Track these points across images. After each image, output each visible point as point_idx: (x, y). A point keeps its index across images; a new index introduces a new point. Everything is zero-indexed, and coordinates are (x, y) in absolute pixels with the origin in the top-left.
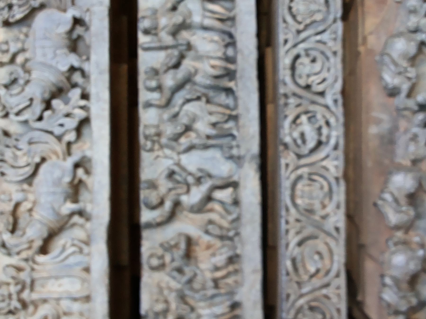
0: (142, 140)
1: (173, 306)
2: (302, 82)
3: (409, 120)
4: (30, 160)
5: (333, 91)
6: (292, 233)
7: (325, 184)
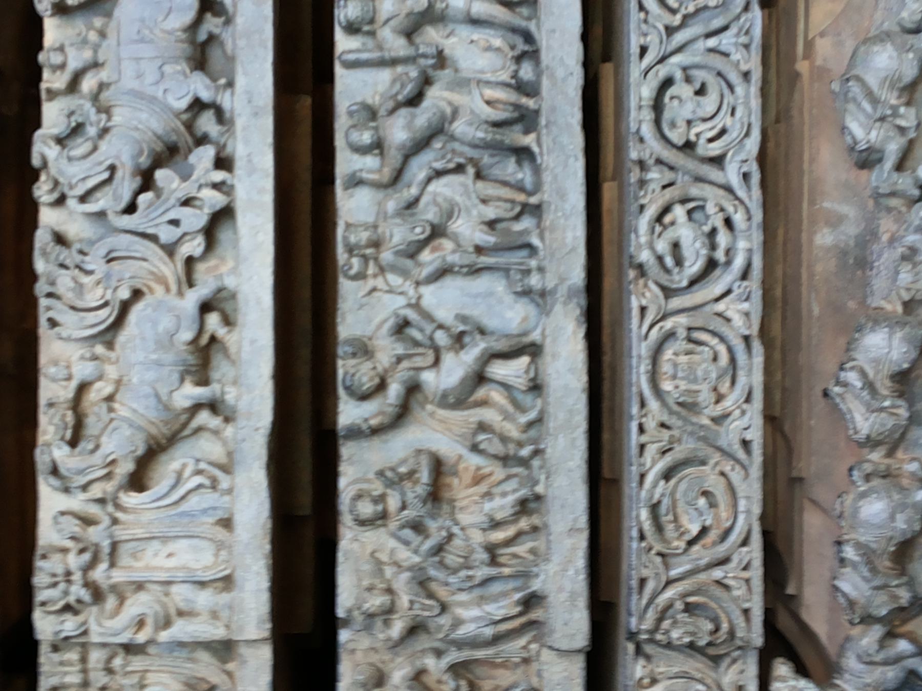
1: (404, 600)
2: (676, 136)
3: (900, 219)
4: (108, 297)
5: (743, 156)
6: (651, 450)
7: (722, 349)
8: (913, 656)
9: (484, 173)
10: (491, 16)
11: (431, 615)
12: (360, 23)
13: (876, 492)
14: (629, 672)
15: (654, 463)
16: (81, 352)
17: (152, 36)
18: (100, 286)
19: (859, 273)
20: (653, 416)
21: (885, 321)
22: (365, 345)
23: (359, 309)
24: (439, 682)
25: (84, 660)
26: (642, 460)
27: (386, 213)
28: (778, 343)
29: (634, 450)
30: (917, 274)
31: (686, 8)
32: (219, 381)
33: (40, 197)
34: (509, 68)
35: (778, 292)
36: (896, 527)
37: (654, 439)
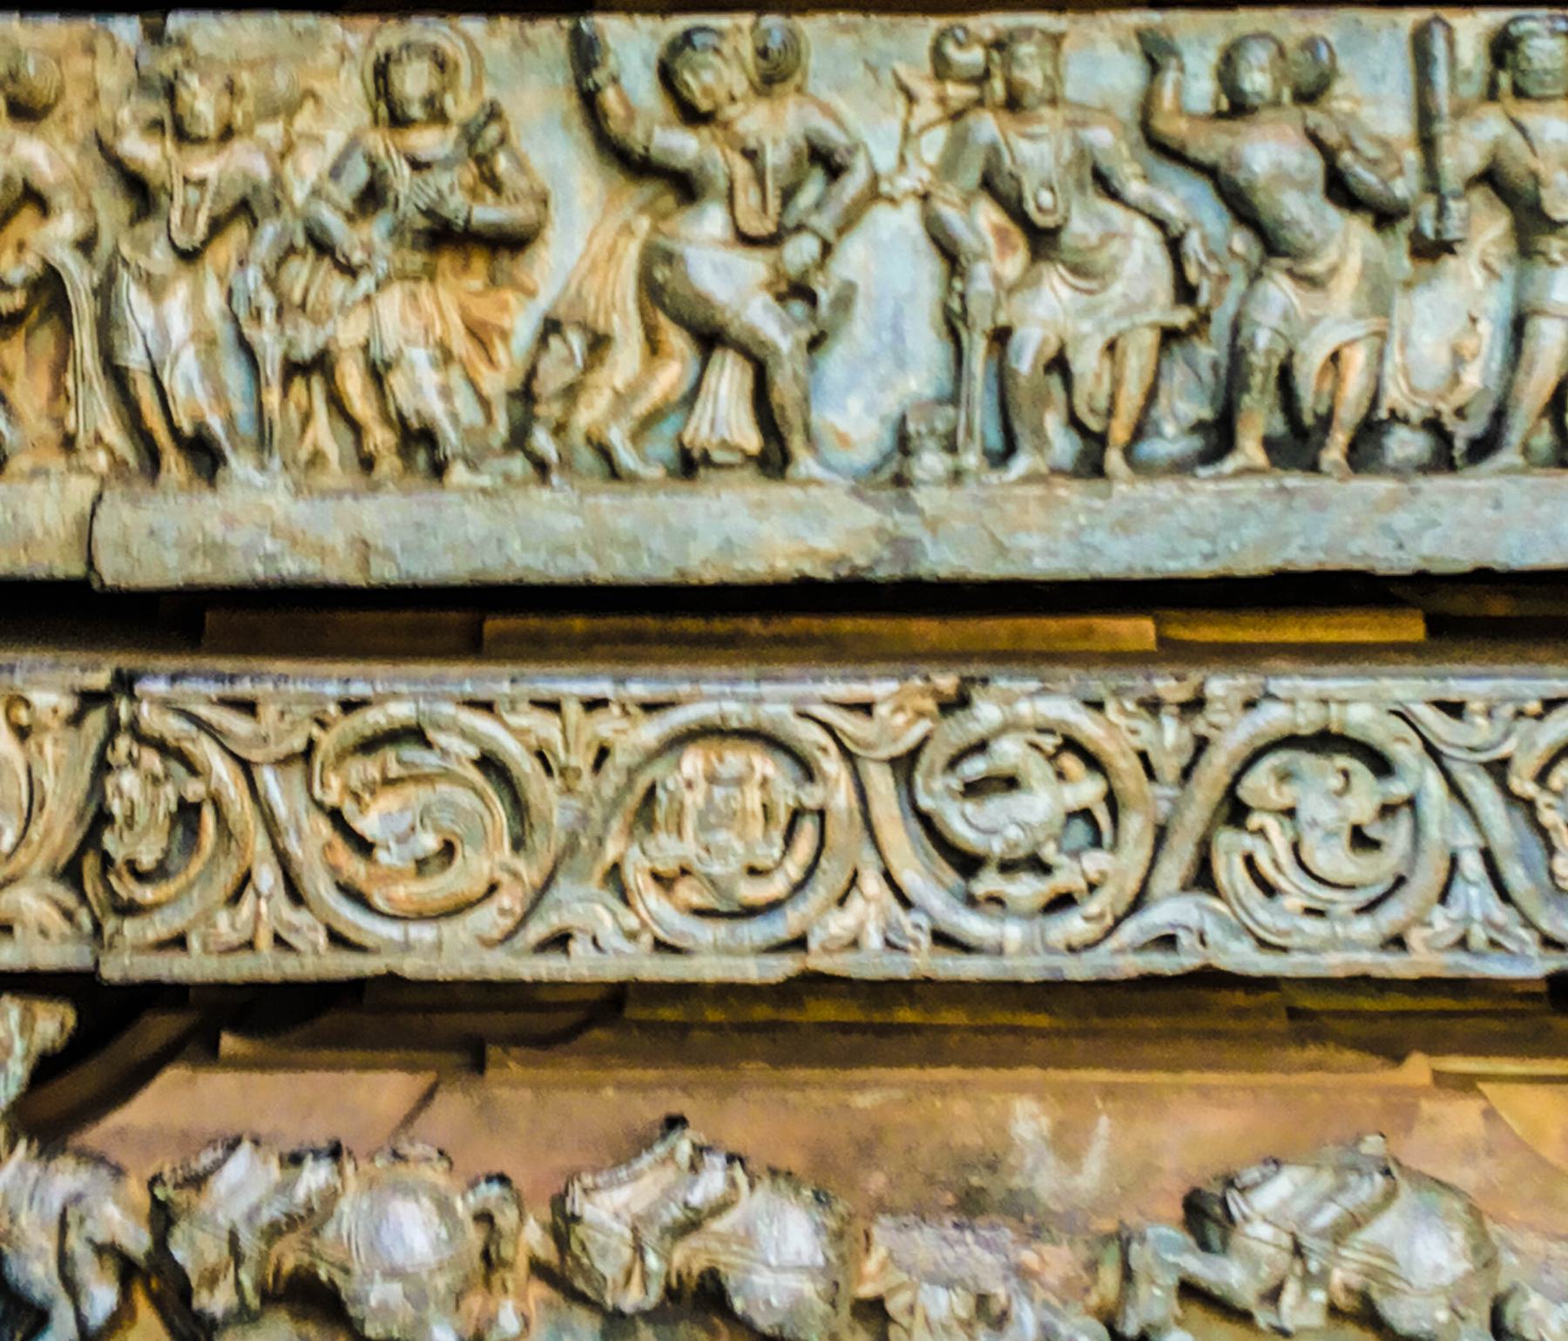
0: (987, 24)
1: (206, 166)
2: (1259, 785)
3: (1072, 1290)
5: (1214, 933)
6: (546, 727)
7: (776, 887)
8: (80, 1320)
9: (1176, 348)
10: (1531, 365)
11: (173, 227)
12: (1516, 67)
13: (451, 1237)
14: (43, 675)
15: (518, 733)
19: (949, 1198)
20: (624, 732)
21: (841, 1257)
22: (784, 79)
23: (867, 65)
24: (21, 246)
26: (524, 706)
27: (1084, 124)
28: (789, 1015)
29: (545, 689)
31: (1550, 806)
34: (1415, 404)
35: (906, 1015)
36: (372, 1281)
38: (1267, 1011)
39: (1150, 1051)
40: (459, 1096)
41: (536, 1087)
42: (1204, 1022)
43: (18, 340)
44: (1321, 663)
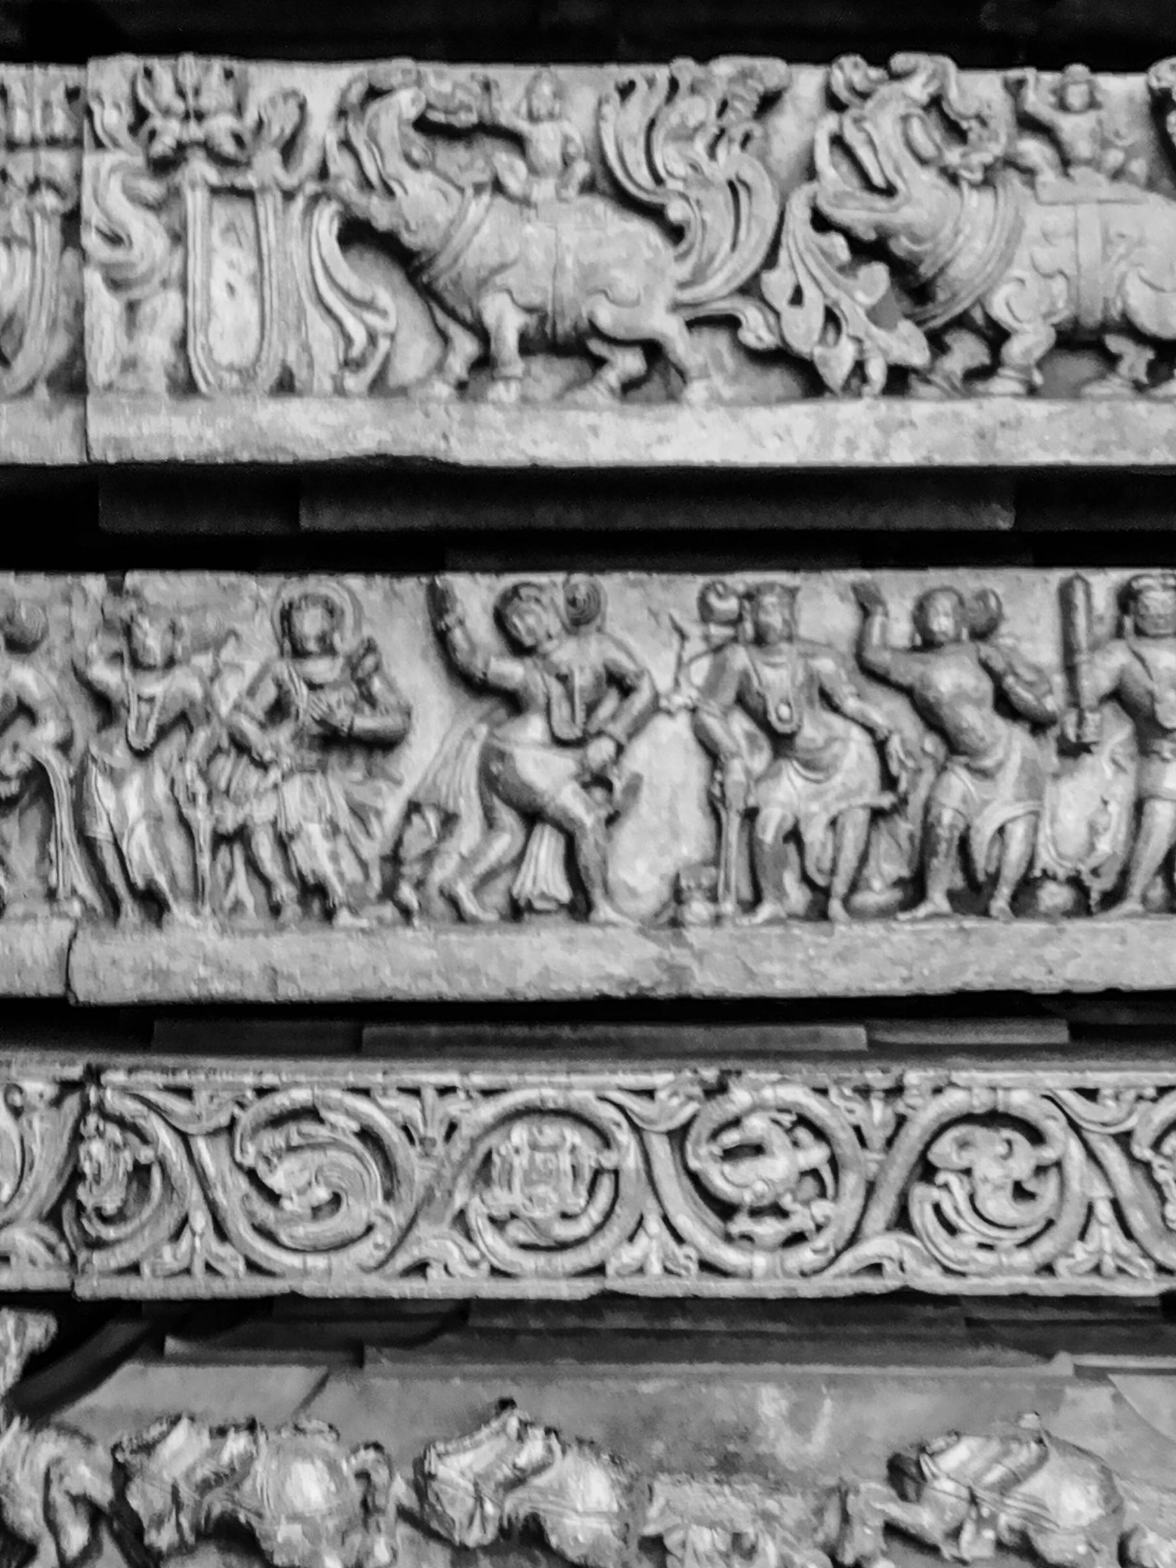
0: (741, 580)
1: (155, 687)
3: (804, 1530)
4: (672, 185)
5: (910, 1263)
6: (410, 1108)
7: (582, 1227)
9: (882, 824)
10: (1149, 835)
12: (1137, 613)
13: (338, 1490)
14: (32, 1068)
15: (389, 1112)
16: (578, 139)
17: (1114, 259)
18: (690, 170)
19: (712, 1461)
20: (468, 1111)
21: (631, 1505)
22: (588, 621)
23: (650, 610)
24: (16, 747)
25: (53, 142)
26: (393, 1092)
27: (813, 656)
28: (592, 1324)
29: (410, 1077)
30: (709, 1559)
31: (1162, 1167)
32: (527, 372)
33: (841, 68)
35: (679, 1324)
36: (279, 1523)
37: (428, 1113)
38: (950, 1321)
39: (862, 1351)
40: (344, 1384)
41: (402, 1377)
42: (903, 1329)
43: (14, 817)
44: (991, 1060)
